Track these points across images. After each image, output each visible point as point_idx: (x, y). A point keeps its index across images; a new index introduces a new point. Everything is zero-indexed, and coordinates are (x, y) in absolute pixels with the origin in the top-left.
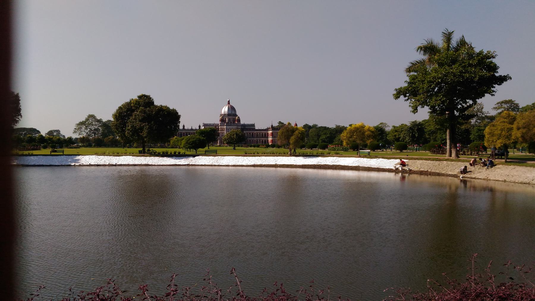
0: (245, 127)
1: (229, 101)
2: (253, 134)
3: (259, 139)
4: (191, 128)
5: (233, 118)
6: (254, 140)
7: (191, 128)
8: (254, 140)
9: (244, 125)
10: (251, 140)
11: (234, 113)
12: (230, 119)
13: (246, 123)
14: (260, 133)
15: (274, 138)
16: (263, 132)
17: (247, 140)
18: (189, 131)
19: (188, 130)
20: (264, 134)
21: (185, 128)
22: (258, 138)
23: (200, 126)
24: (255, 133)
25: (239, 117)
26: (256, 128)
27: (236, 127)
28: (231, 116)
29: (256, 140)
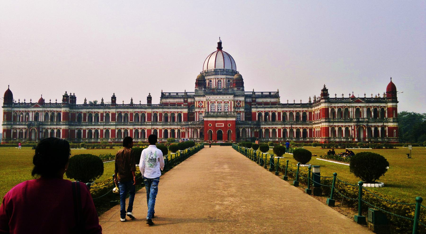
0: (254, 99)
1: (220, 44)
2: (274, 114)
3: (290, 126)
4: (130, 103)
5: (226, 78)
6: (277, 130)
7: (130, 103)
8: (277, 130)
9: (253, 96)
10: (271, 130)
13: (259, 89)
14: (291, 113)
15: (331, 124)
17: (261, 130)
18: (126, 110)
19: (124, 106)
20: (301, 114)
21: (119, 102)
22: (287, 124)
23: (149, 99)
24: (279, 114)
26: (283, 101)
27: (231, 97)
29: (282, 130)
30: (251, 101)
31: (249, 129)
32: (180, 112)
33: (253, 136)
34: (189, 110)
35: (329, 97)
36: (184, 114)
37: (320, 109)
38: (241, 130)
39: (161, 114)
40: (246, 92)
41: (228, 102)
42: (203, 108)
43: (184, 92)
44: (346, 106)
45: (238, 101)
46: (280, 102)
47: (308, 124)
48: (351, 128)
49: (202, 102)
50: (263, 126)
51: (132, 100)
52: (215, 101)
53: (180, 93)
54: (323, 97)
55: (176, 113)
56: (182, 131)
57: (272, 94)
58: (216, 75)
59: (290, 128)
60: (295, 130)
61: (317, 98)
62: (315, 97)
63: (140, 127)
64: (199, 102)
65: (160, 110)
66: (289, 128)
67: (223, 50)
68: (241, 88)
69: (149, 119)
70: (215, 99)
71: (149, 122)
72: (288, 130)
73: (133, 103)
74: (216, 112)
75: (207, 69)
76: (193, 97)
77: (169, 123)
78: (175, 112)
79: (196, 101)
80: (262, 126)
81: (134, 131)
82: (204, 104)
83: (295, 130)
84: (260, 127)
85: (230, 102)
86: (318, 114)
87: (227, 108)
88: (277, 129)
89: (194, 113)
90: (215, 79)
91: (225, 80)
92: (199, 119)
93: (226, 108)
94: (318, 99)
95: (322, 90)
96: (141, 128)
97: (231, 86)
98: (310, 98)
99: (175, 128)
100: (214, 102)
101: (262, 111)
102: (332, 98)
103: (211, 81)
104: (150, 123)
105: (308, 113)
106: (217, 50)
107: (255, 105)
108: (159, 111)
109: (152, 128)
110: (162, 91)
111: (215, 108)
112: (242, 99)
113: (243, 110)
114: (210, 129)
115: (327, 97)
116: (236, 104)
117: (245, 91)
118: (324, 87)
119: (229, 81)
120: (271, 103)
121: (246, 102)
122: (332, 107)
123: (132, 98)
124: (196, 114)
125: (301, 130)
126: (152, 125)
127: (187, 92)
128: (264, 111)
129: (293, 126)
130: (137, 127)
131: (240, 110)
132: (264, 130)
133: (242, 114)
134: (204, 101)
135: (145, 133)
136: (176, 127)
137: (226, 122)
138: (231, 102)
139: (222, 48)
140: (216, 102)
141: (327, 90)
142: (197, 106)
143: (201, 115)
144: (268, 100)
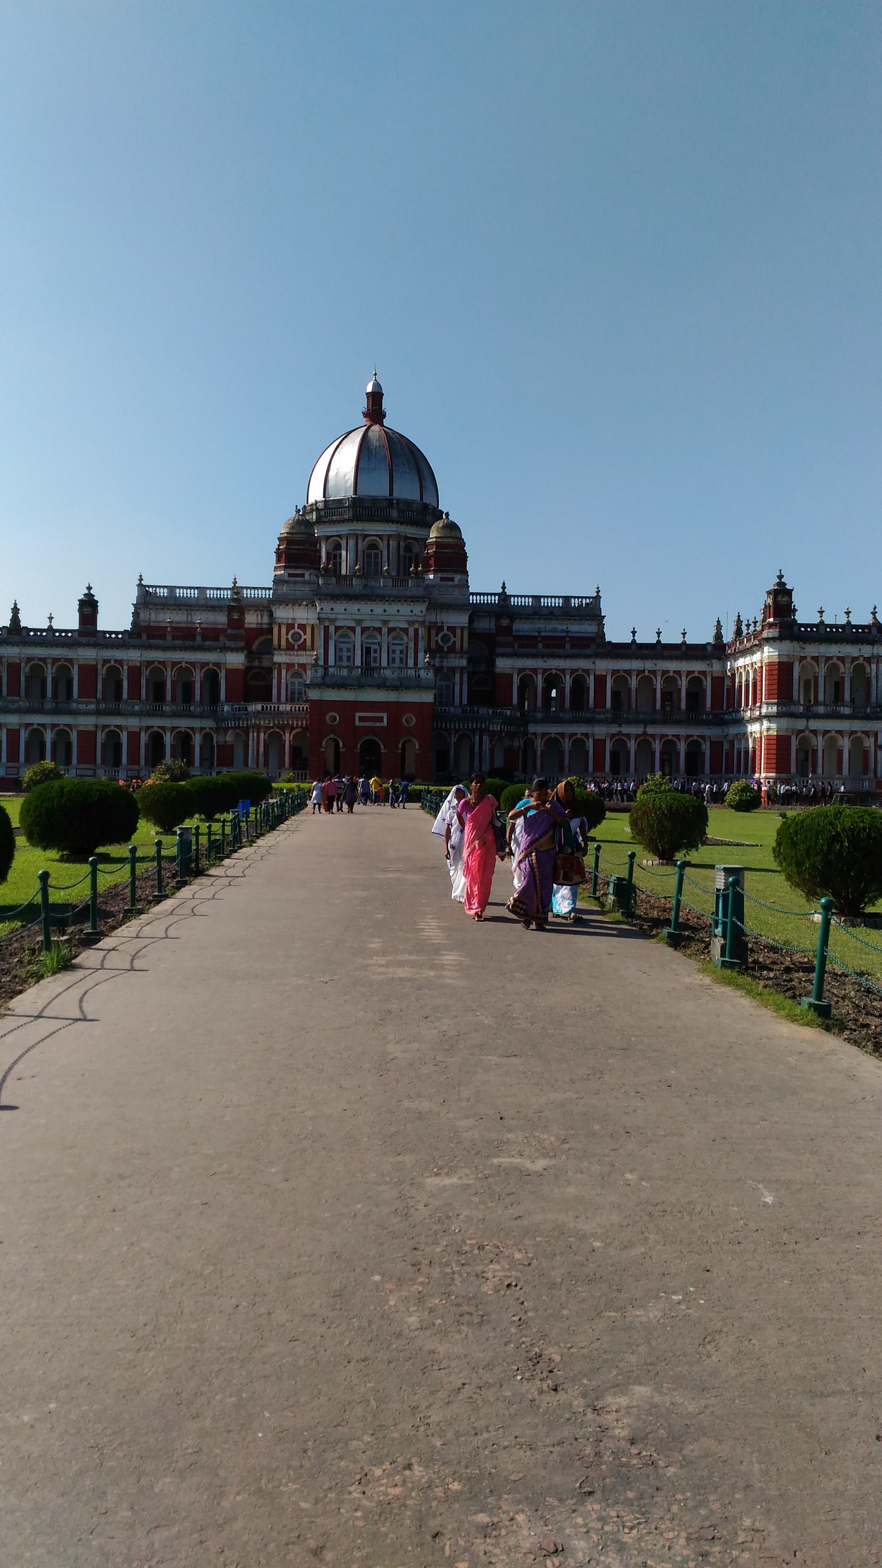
0: (505, 622)
3: (638, 730)
4: (7, 623)
5: (398, 537)
6: (590, 744)
8: (590, 744)
10: (567, 745)
11: (416, 497)
12: (373, 546)
14: (646, 680)
15: (801, 724)
16: (672, 666)
17: (529, 744)
20: (683, 683)
22: (629, 722)
24: (600, 681)
25: (453, 527)
27: (419, 609)
28: (388, 520)
29: (609, 746)
30: (494, 632)
31: (486, 739)
32: (214, 664)
33: (499, 763)
34: (250, 657)
35: (795, 620)
36: (228, 671)
37: (759, 665)
38: (454, 739)
39: (135, 672)
40: (476, 594)
41: (405, 631)
42: (303, 653)
43: (231, 586)
44: (857, 658)
45: (445, 629)
46: (603, 635)
47: (708, 723)
48: (872, 740)
49: (302, 627)
50: (539, 729)
51: (15, 610)
52: (353, 624)
53: (213, 589)
54: (771, 620)
55: (198, 670)
56: (222, 739)
57: (575, 603)
58: (356, 518)
59: (642, 738)
60: (657, 746)
61: (748, 626)
62: (739, 622)
63: (47, 720)
64: (290, 627)
65: (134, 656)
66: (638, 736)
67: (386, 422)
68: (457, 577)
69: (87, 690)
70: (354, 617)
71: (87, 703)
72: (632, 746)
73: (23, 624)
74: (358, 667)
75: (324, 496)
76: (265, 607)
77: (166, 708)
78: (193, 664)
79: (279, 621)
80: (532, 728)
81: (23, 735)
82: (308, 637)
83: (657, 746)
84: (526, 733)
85: (411, 632)
86: (747, 686)
87: (401, 652)
88: (591, 741)
89: (270, 670)
90: (357, 537)
91: (393, 544)
92: (289, 697)
93: (398, 652)
94: (752, 628)
95: (769, 593)
96: (54, 726)
97: (416, 567)
98: (719, 626)
99: (192, 729)
100: (349, 628)
101: (535, 671)
102: (806, 626)
103: (338, 547)
104: (92, 707)
105: (708, 684)
106: (364, 421)
107: (511, 645)
108: (125, 658)
109: (96, 726)
110: (141, 579)
111: (350, 654)
112: (461, 619)
113: (464, 663)
114: (332, 736)
115: (787, 619)
116: (434, 638)
117: (471, 590)
118: (778, 580)
119: (408, 549)
120: (570, 637)
121: (473, 635)
122: (805, 657)
123: (15, 604)
124: (276, 672)
125: (682, 747)
126: (98, 713)
127: (242, 588)
128: (545, 670)
129: (650, 730)
130: (36, 719)
131: (452, 665)
132: (539, 744)
133: (457, 676)
134: (311, 622)
135: (69, 745)
136: (196, 723)
137: (395, 709)
138: (416, 631)
139: (384, 416)
140: (358, 630)
141: (789, 593)
142: (283, 643)
143: (296, 681)
144: (560, 627)
